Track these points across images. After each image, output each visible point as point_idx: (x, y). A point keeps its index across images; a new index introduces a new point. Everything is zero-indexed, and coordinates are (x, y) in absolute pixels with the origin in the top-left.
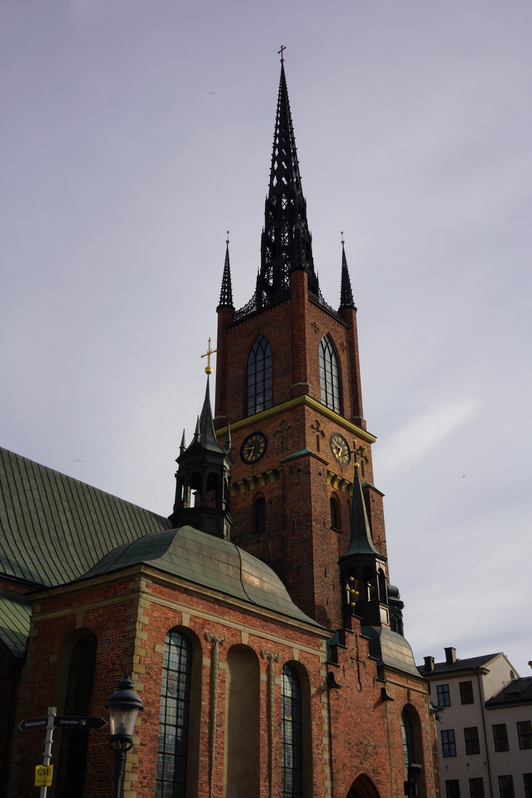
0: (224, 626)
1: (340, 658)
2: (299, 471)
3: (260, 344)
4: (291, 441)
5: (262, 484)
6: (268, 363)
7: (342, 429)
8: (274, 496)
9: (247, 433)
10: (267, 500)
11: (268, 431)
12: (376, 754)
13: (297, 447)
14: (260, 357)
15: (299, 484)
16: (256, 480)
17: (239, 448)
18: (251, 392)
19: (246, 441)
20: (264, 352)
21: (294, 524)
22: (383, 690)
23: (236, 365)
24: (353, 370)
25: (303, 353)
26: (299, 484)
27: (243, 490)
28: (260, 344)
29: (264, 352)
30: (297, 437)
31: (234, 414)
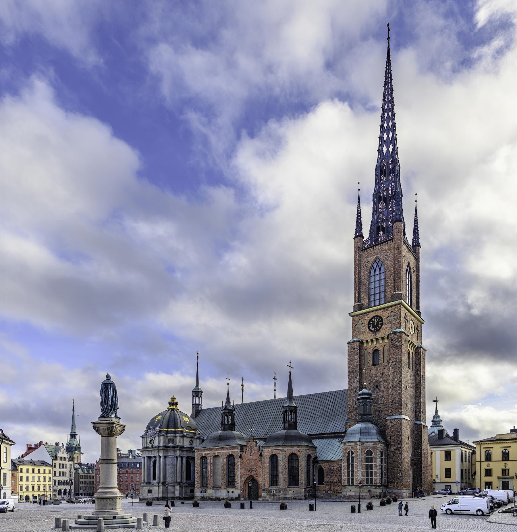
22: (261, 453)
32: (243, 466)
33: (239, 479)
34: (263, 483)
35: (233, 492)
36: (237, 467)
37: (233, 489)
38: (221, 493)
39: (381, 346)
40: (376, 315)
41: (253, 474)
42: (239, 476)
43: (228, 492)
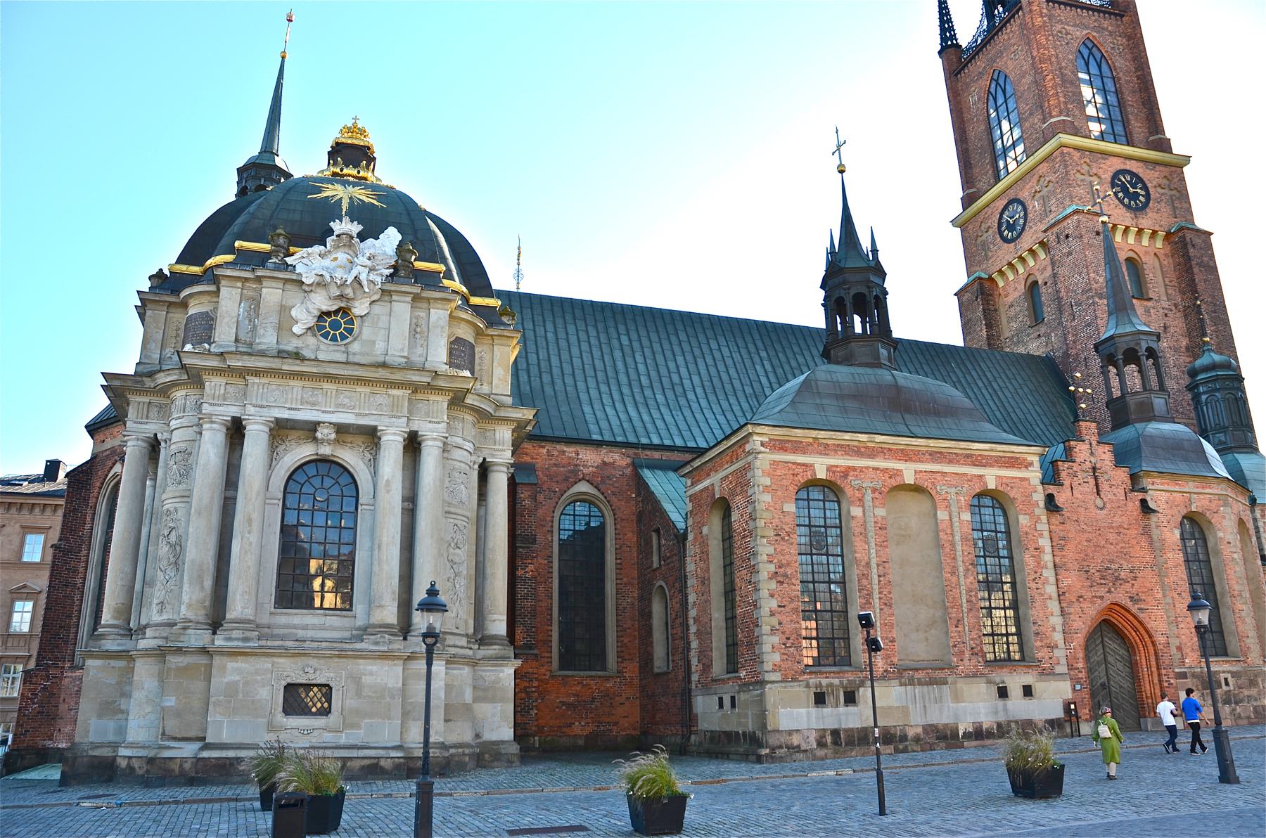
0: (876, 469)
1: (1063, 475)
3: (998, 84)
5: (1031, 263)
6: (1011, 105)
7: (1128, 162)
9: (1001, 203)
11: (1024, 195)
12: (1135, 578)
14: (1000, 100)
15: (1070, 253)
16: (1022, 259)
20: (1004, 92)
22: (1144, 502)
26: (1070, 253)
27: (1011, 277)
28: (998, 84)
29: (1004, 92)
32: (1070, 553)
33: (1056, 620)
34: (1174, 643)
35: (1028, 691)
36: (1038, 559)
37: (1028, 679)
38: (957, 698)
39: (1146, 253)
40: (1128, 168)
41: (1121, 597)
42: (1054, 606)
43: (1003, 693)
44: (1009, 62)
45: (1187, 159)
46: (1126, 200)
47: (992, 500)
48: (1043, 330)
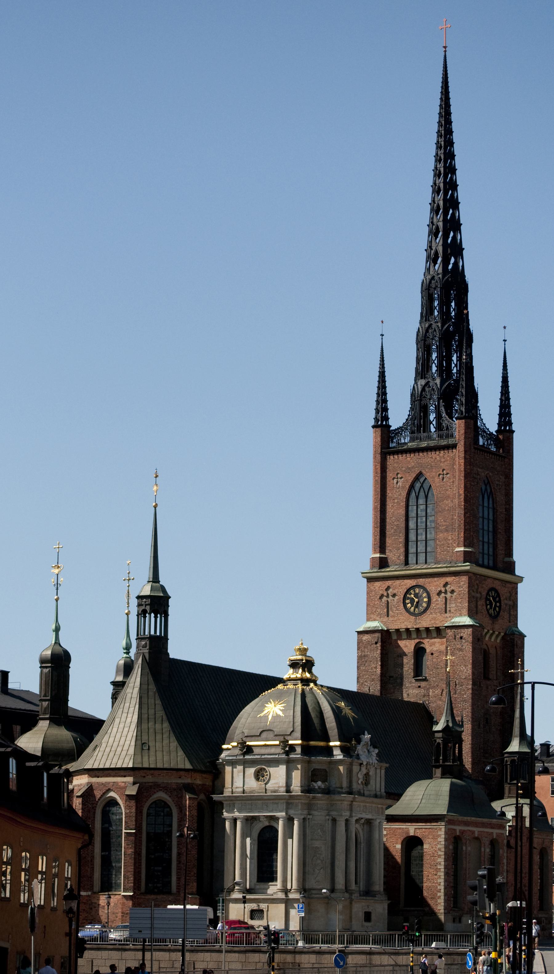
2: (461, 638)
4: (454, 605)
8: (435, 649)
10: (428, 651)
13: (460, 612)
17: (402, 597)
18: (412, 536)
19: (408, 591)
20: (426, 497)
21: (456, 684)
23: (396, 501)
24: (508, 506)
25: (468, 515)
26: (461, 650)
29: (426, 497)
30: (460, 603)
31: (395, 555)
36: (503, 867)
44: (437, 480)
45: (521, 579)
46: (489, 606)
47: (493, 843)
48: (423, 684)
